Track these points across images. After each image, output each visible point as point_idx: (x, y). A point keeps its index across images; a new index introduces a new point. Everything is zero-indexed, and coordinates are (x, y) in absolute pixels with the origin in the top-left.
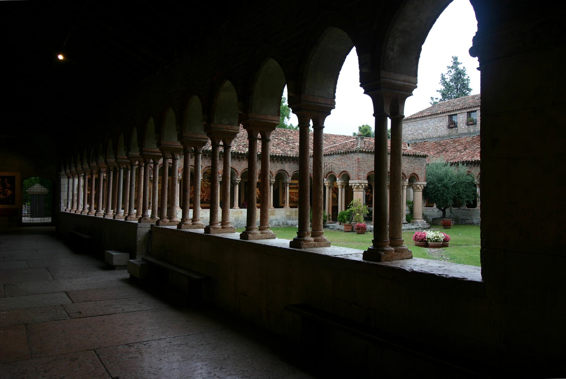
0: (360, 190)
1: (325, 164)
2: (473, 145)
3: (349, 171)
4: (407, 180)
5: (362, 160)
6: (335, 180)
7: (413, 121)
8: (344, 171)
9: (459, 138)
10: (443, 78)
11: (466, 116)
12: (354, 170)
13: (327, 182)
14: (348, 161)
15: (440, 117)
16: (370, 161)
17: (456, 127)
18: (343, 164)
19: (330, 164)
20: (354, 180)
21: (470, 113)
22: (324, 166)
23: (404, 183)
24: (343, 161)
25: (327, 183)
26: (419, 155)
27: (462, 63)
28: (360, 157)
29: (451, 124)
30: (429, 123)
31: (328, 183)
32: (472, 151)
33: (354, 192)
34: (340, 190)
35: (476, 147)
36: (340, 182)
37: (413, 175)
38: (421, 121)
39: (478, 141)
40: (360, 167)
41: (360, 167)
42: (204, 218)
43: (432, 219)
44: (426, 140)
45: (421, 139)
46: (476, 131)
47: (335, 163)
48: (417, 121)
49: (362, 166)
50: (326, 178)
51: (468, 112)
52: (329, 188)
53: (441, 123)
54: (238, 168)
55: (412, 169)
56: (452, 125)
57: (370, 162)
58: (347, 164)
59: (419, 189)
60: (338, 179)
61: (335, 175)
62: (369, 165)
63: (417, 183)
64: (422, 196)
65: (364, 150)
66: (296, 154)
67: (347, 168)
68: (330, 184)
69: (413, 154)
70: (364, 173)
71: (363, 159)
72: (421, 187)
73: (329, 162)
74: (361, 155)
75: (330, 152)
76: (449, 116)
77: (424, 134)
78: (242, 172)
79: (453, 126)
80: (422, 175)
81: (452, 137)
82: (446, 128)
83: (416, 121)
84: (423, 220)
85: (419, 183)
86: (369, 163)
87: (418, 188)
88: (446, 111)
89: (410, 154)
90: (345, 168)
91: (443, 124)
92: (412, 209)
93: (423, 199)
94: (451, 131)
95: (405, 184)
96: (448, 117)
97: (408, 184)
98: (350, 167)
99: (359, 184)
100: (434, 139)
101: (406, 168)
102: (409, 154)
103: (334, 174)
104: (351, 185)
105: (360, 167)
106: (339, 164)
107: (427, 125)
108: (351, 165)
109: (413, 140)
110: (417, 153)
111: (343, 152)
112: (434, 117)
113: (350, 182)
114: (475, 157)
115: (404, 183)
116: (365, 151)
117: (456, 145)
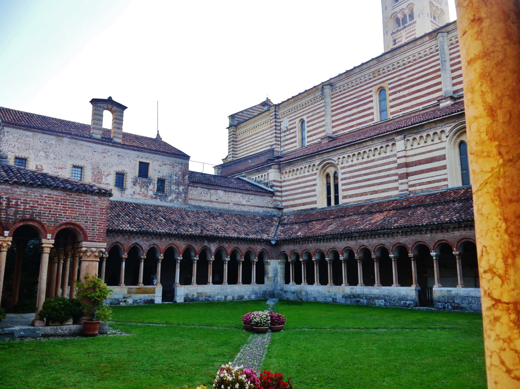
3: (82, 224)
12: (96, 225)
20: (96, 242)
58: (78, 212)
90: (74, 219)
98: (87, 217)
108: (89, 215)
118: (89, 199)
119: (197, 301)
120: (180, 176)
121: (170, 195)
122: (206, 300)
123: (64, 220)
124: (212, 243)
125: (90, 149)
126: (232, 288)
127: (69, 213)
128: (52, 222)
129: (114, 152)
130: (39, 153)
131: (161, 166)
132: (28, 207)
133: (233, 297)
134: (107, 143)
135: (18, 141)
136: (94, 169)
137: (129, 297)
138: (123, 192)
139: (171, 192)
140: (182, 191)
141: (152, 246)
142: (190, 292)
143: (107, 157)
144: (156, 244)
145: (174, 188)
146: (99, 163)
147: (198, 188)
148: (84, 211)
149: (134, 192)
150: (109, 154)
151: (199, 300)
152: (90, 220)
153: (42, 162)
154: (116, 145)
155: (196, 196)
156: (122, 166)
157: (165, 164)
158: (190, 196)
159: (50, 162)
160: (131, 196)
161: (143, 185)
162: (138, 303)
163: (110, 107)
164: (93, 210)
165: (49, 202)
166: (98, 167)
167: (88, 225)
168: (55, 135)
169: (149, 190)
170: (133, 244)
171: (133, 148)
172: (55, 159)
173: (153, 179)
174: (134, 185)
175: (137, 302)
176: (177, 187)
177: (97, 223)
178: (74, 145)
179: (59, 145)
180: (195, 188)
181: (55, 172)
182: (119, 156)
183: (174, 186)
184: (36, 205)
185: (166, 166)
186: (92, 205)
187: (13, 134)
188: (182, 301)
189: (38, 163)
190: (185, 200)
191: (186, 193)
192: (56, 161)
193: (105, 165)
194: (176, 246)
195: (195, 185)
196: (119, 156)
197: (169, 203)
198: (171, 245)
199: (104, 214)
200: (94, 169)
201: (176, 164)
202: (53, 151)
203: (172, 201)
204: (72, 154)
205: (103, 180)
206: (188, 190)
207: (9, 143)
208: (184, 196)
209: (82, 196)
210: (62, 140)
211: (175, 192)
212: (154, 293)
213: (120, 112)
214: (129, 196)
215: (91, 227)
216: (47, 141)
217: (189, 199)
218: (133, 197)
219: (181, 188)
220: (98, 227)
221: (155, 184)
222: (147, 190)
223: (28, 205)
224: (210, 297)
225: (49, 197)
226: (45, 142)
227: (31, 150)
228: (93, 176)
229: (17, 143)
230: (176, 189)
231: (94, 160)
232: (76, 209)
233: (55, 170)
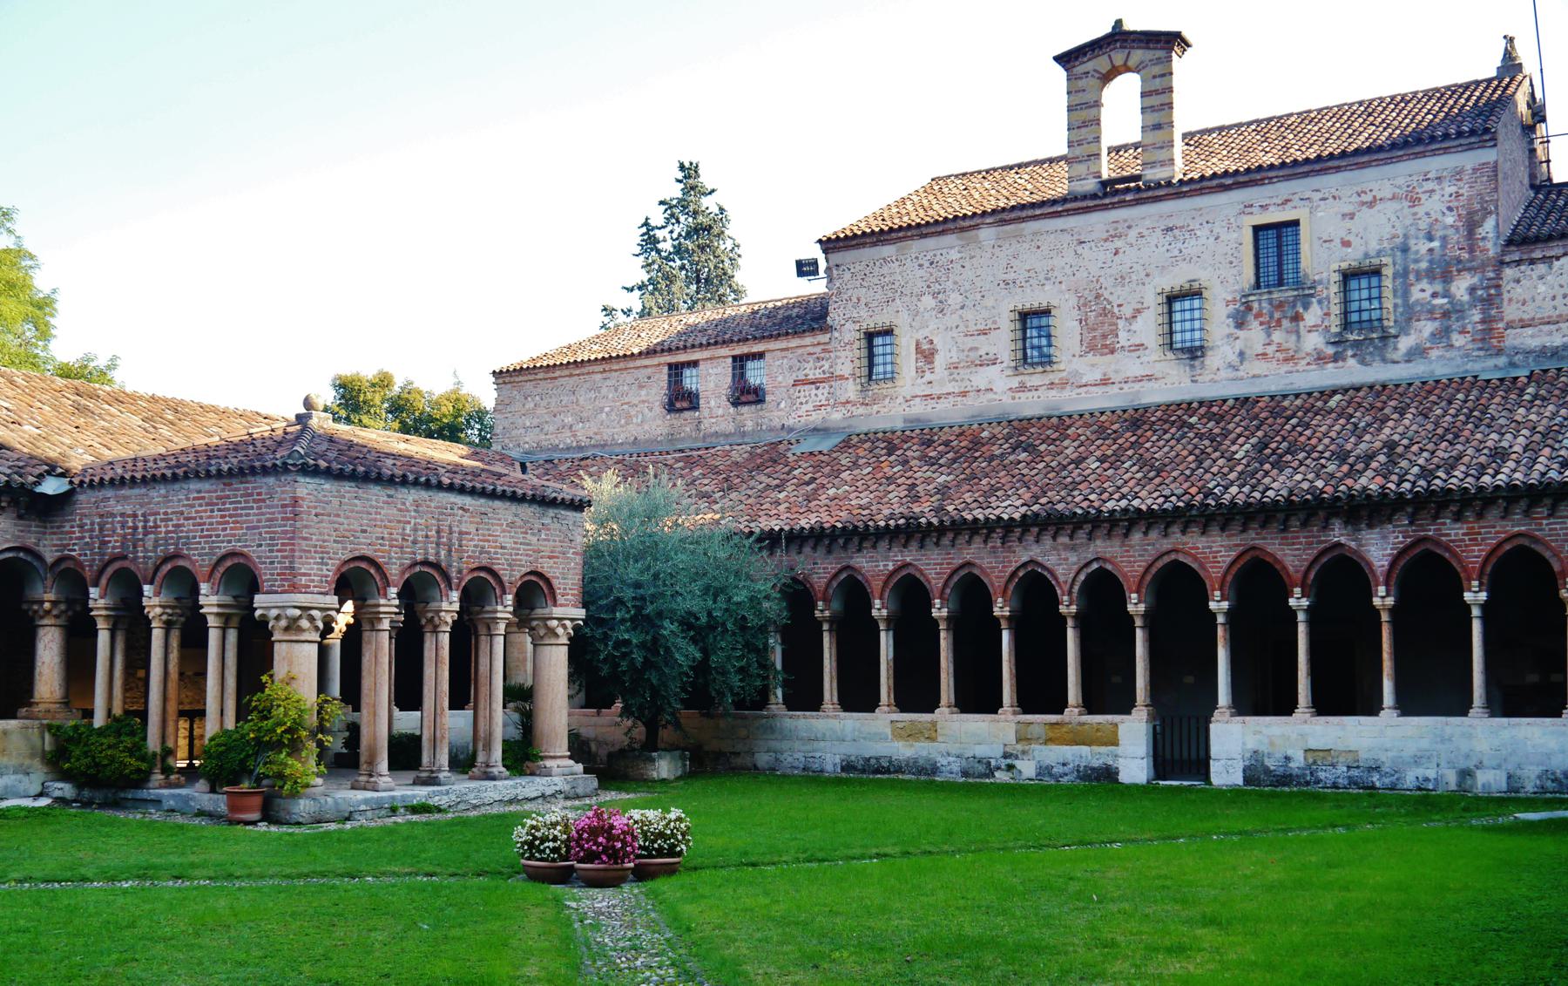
0: (302, 638)
1: (146, 521)
2: (753, 477)
4: (509, 599)
5: (316, 507)
6: (195, 591)
7: (538, 377)
8: (233, 554)
9: (707, 449)
10: (650, 241)
11: (730, 369)
12: (278, 551)
13: (156, 601)
14: (252, 508)
15: (638, 368)
16: (352, 511)
17: (695, 407)
18: (228, 523)
19: (171, 520)
20: (276, 592)
21: (741, 360)
22: (145, 527)
23: (496, 612)
24: (228, 509)
25: (155, 606)
26: (555, 498)
27: (713, 191)
28: (306, 491)
29: (677, 399)
30: (598, 389)
31: (160, 606)
32: (750, 496)
33: (277, 646)
34: (213, 636)
35: (764, 485)
36: (214, 599)
37: (533, 578)
38: (572, 381)
39: (770, 464)
40: (305, 539)
41: (305, 539)
43: (606, 752)
44: (589, 454)
45: (568, 449)
46: (764, 427)
47: (195, 518)
48: (555, 378)
49: (311, 531)
50: (151, 583)
51: (735, 358)
52: (168, 626)
53: (643, 392)
55: (527, 555)
56: (681, 400)
58: (245, 522)
59: (557, 636)
60: (204, 588)
61: (194, 571)
62: (346, 530)
63: (546, 611)
64: (567, 663)
65: (323, 464)
66: (8, 471)
67: (246, 540)
68: (169, 611)
69: (533, 495)
70: (322, 564)
71: (321, 502)
72: (565, 627)
73: (166, 513)
74: (310, 486)
75: (170, 468)
76: (670, 366)
77: (583, 428)
79: (685, 405)
80: (567, 578)
81: (680, 447)
82: (658, 409)
83: (551, 378)
84: (571, 762)
85: (557, 612)
86: (345, 522)
87: (552, 633)
88: (659, 348)
89: (520, 492)
90: (239, 541)
91: (648, 394)
92: (528, 723)
93: (570, 675)
94: (675, 422)
95: (499, 615)
96: (666, 370)
97: (510, 616)
98: (260, 534)
99: (298, 612)
100: (617, 450)
101: (502, 548)
102: (514, 492)
103: (190, 568)
104: (262, 615)
106: (211, 524)
107: (592, 395)
108: (264, 527)
109: (542, 449)
110: (551, 490)
111: (230, 469)
112: (615, 367)
113: (259, 600)
114: (760, 520)
115: (496, 612)
116: (328, 468)
117: (696, 474)
118: (261, 487)
119: (1308, 783)
120: (1451, 232)
121: (1404, 329)
122: (1353, 782)
123: (225, 547)
124: (1370, 526)
125: (1066, 238)
126: (1506, 735)
127: (232, 529)
128: (206, 554)
129: (1148, 223)
130: (919, 304)
131: (1352, 216)
132: (170, 528)
133: (1509, 777)
134: (1116, 199)
135: (865, 284)
136: (1085, 305)
137: (1024, 752)
138: (1197, 363)
139: (1409, 315)
140: (1466, 298)
141: (1095, 566)
142: (1272, 744)
143: (1127, 248)
144: (1108, 555)
145: (1427, 295)
146: (1102, 280)
147: (1557, 264)
148: (255, 518)
149: (1241, 354)
150: (1133, 234)
151: (1318, 781)
152: (265, 539)
153: (931, 328)
154: (1150, 194)
155: (1549, 304)
156: (1183, 265)
157: (1371, 204)
158: (1511, 312)
159: (951, 320)
160: (1231, 374)
161: (1277, 315)
162: (1057, 778)
163: (1118, 58)
164: (270, 513)
165: (200, 509)
166: (1098, 296)
167: (262, 552)
168: (952, 231)
169: (1303, 331)
170: (1024, 565)
171: (1215, 182)
172: (962, 308)
173: (1320, 282)
174: (1240, 325)
175: (1051, 775)
176: (1438, 287)
177: (277, 544)
178: (1014, 241)
179: (972, 258)
180: (1541, 268)
181: (971, 349)
182: (1171, 229)
183: (1424, 284)
184: (182, 522)
185: (1379, 207)
186: (268, 502)
187: (851, 267)
188: (1238, 779)
189: (920, 335)
190: (1488, 337)
191: (1489, 299)
192: (969, 314)
193: (1122, 279)
194: (1196, 559)
195: (1537, 254)
196: (1171, 229)
197: (1402, 365)
198: (1173, 556)
199: (288, 519)
200: (1085, 305)
201: (1429, 185)
202: (956, 283)
203: (1417, 353)
204: (1011, 276)
205: (1123, 335)
206: (1498, 287)
207: (846, 297)
208: (1477, 317)
209: (246, 483)
210: (977, 241)
211: (1431, 312)
212: (1115, 743)
213: (1159, 61)
214: (1223, 374)
215: (268, 558)
216: (937, 259)
217: (1509, 326)
218: (1240, 374)
219: (1461, 287)
220: (279, 554)
221: (1328, 298)
222: (1298, 333)
223: (170, 523)
224: (1377, 769)
225: (198, 498)
226: (932, 263)
227: (898, 301)
228: (1085, 332)
229: (864, 290)
230: (1434, 295)
231: (1082, 274)
232: (241, 515)
233: (970, 342)
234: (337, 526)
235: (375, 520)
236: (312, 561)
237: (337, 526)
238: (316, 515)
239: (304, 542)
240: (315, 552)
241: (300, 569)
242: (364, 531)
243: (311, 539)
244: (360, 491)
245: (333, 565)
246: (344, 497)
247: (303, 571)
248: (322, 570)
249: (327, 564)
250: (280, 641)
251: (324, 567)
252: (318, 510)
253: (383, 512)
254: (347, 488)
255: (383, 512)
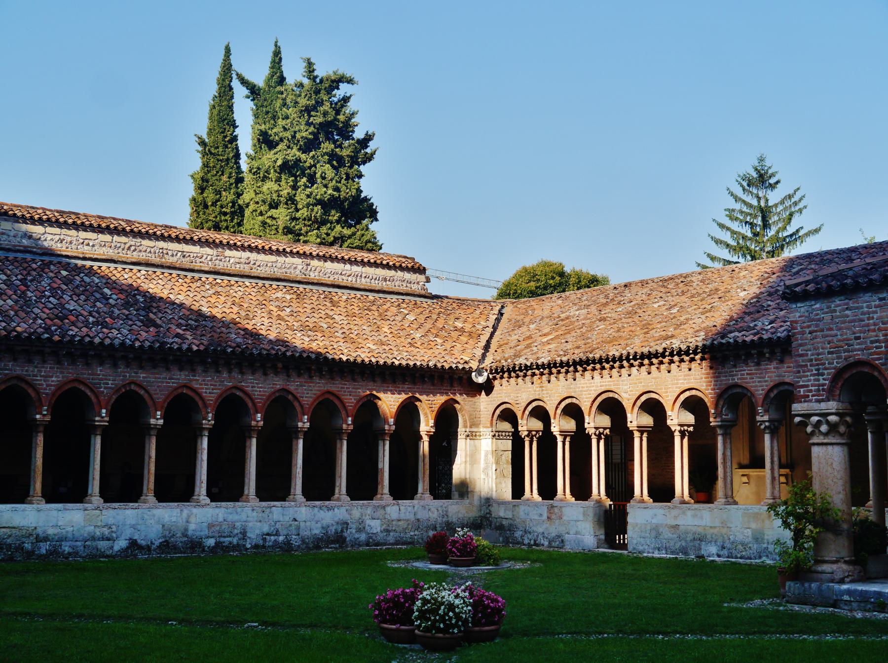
5: (809, 327)
16: (844, 322)
28: (798, 314)
40: (802, 355)
41: (802, 355)
42: (682, 528)
49: (805, 348)
54: (756, 386)
57: (839, 329)
62: (839, 341)
70: (818, 374)
71: (813, 320)
74: (802, 310)
78: (767, 395)
105: (801, 352)
234: (830, 339)
235: (868, 325)
236: (809, 374)
237: (830, 339)
238: (810, 333)
239: (800, 359)
240: (811, 366)
241: (799, 382)
242: (859, 338)
243: (807, 355)
244: (851, 302)
245: (828, 374)
246: (835, 311)
247: (801, 383)
248: (819, 380)
249: (823, 374)
250: (814, 444)
251: (821, 378)
252: (812, 328)
253: (875, 316)
254: (837, 303)
255: (875, 316)
